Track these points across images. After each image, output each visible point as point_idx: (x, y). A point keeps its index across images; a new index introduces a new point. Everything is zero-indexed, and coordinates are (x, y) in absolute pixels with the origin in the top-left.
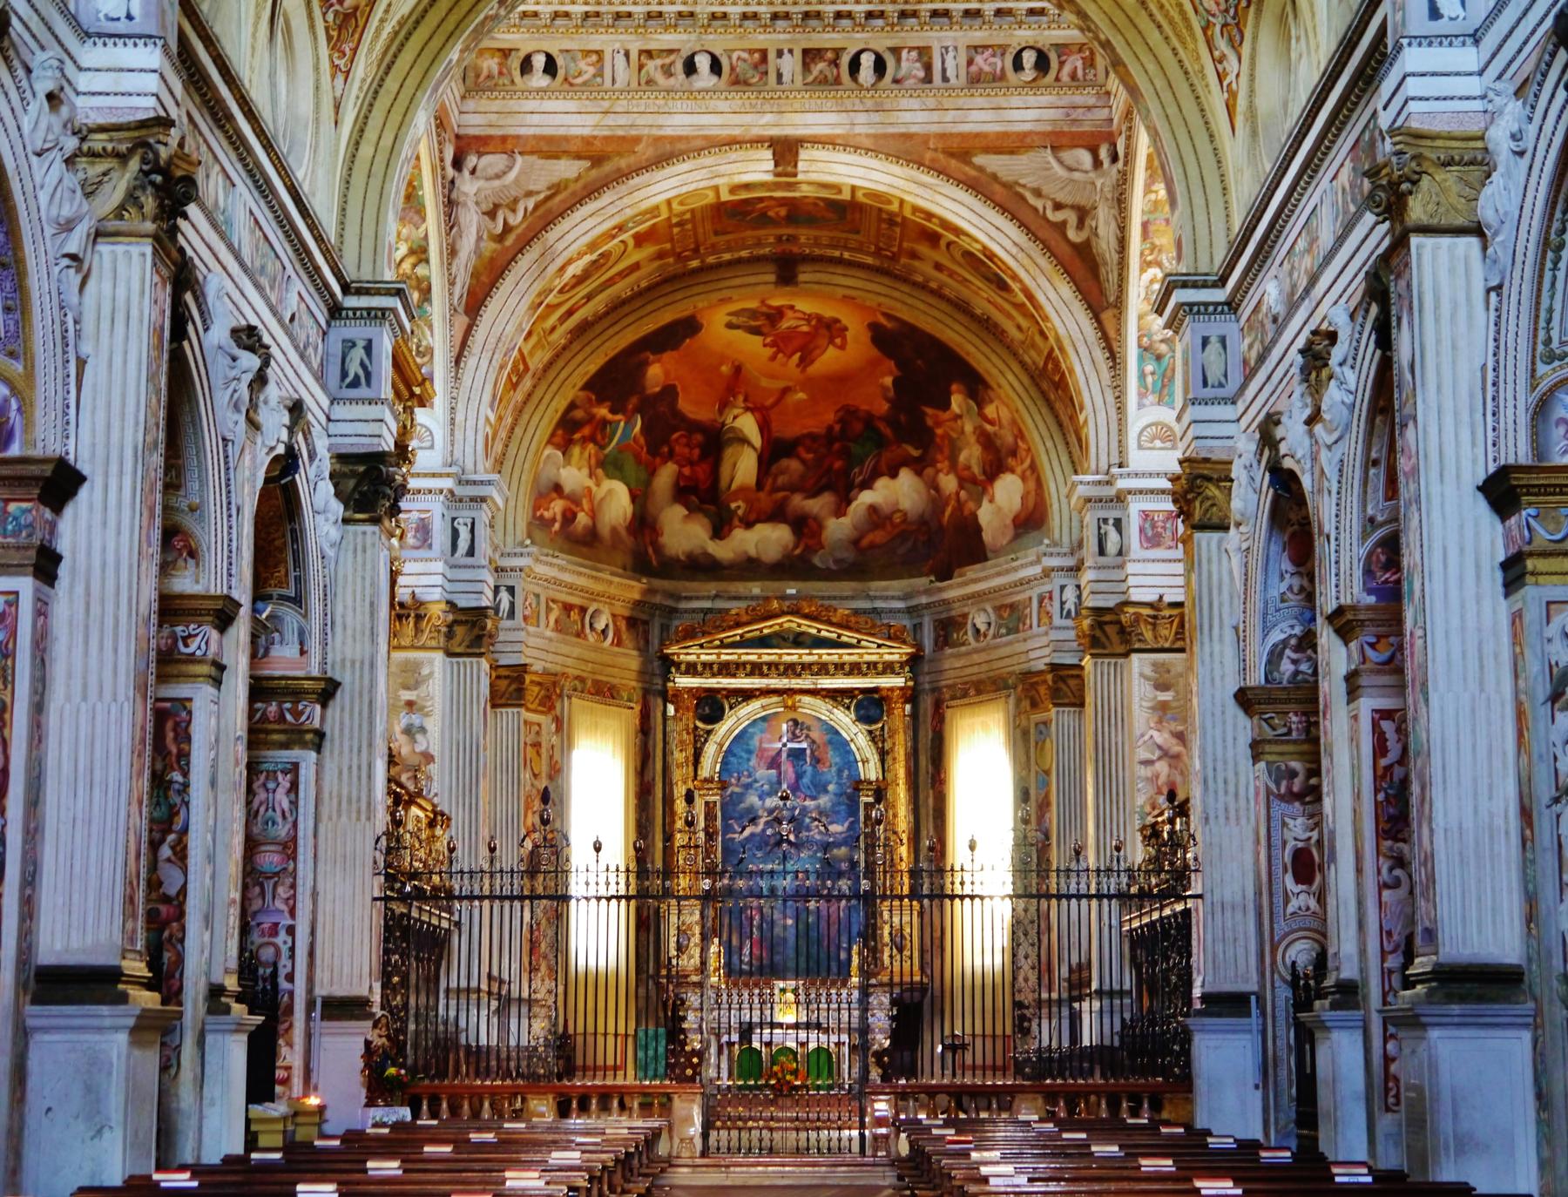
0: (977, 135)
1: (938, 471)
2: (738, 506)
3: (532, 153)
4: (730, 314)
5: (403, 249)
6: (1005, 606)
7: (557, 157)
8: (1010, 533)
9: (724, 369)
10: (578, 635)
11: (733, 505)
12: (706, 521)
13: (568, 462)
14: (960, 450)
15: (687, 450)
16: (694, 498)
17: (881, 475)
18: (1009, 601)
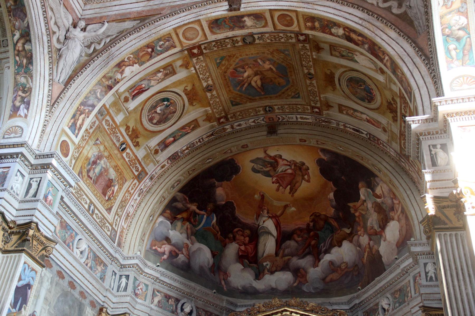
1: (359, 237)
2: (267, 264)
3: (113, 21)
4: (252, 161)
5: (17, 35)
6: (397, 291)
7: (124, 21)
8: (396, 251)
9: (257, 196)
10: (173, 312)
11: (265, 264)
12: (252, 272)
13: (174, 228)
14: (368, 219)
15: (242, 238)
16: (246, 261)
17: (335, 246)
18: (398, 287)
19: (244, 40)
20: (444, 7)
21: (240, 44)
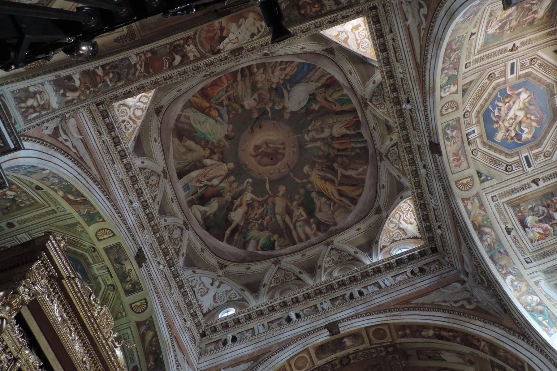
0: (409, 295)
3: (228, 367)
19: (341, 362)
20: (516, 292)
21: (338, 366)
